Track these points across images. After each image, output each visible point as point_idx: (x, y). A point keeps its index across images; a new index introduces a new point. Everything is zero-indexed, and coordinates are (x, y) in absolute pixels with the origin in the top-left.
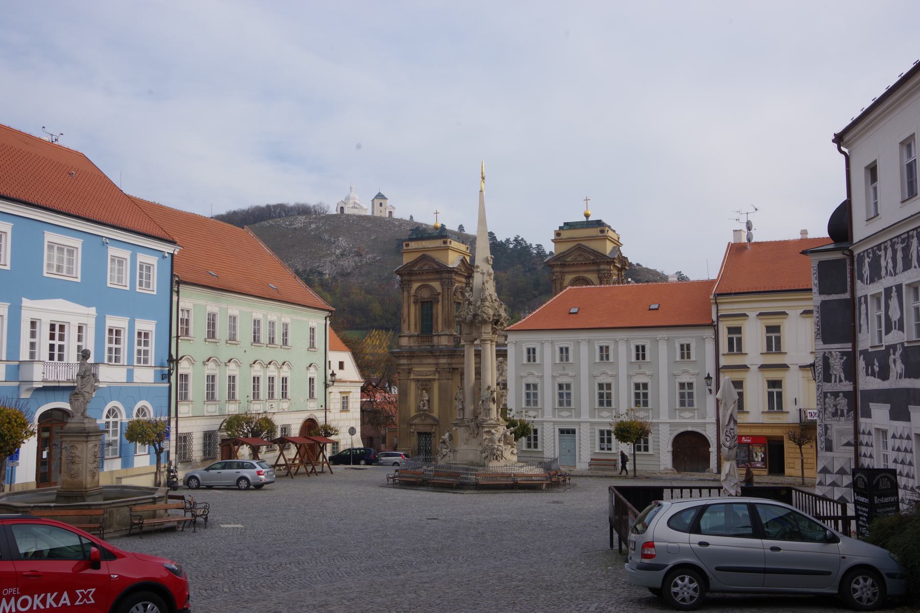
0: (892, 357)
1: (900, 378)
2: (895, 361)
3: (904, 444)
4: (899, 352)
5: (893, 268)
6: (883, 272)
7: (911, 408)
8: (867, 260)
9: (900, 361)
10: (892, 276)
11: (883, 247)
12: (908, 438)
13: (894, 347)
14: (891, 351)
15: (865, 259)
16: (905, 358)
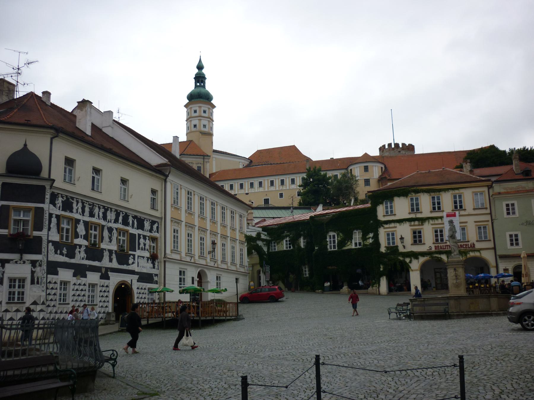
0: (78, 250)
1: (82, 259)
2: (80, 252)
3: (81, 287)
4: (83, 249)
5: (82, 212)
6: (74, 210)
7: (87, 272)
8: (60, 199)
9: (84, 252)
10: (81, 215)
11: (75, 199)
12: (84, 285)
13: (80, 246)
14: (78, 247)
15: (59, 197)
16: (86, 252)
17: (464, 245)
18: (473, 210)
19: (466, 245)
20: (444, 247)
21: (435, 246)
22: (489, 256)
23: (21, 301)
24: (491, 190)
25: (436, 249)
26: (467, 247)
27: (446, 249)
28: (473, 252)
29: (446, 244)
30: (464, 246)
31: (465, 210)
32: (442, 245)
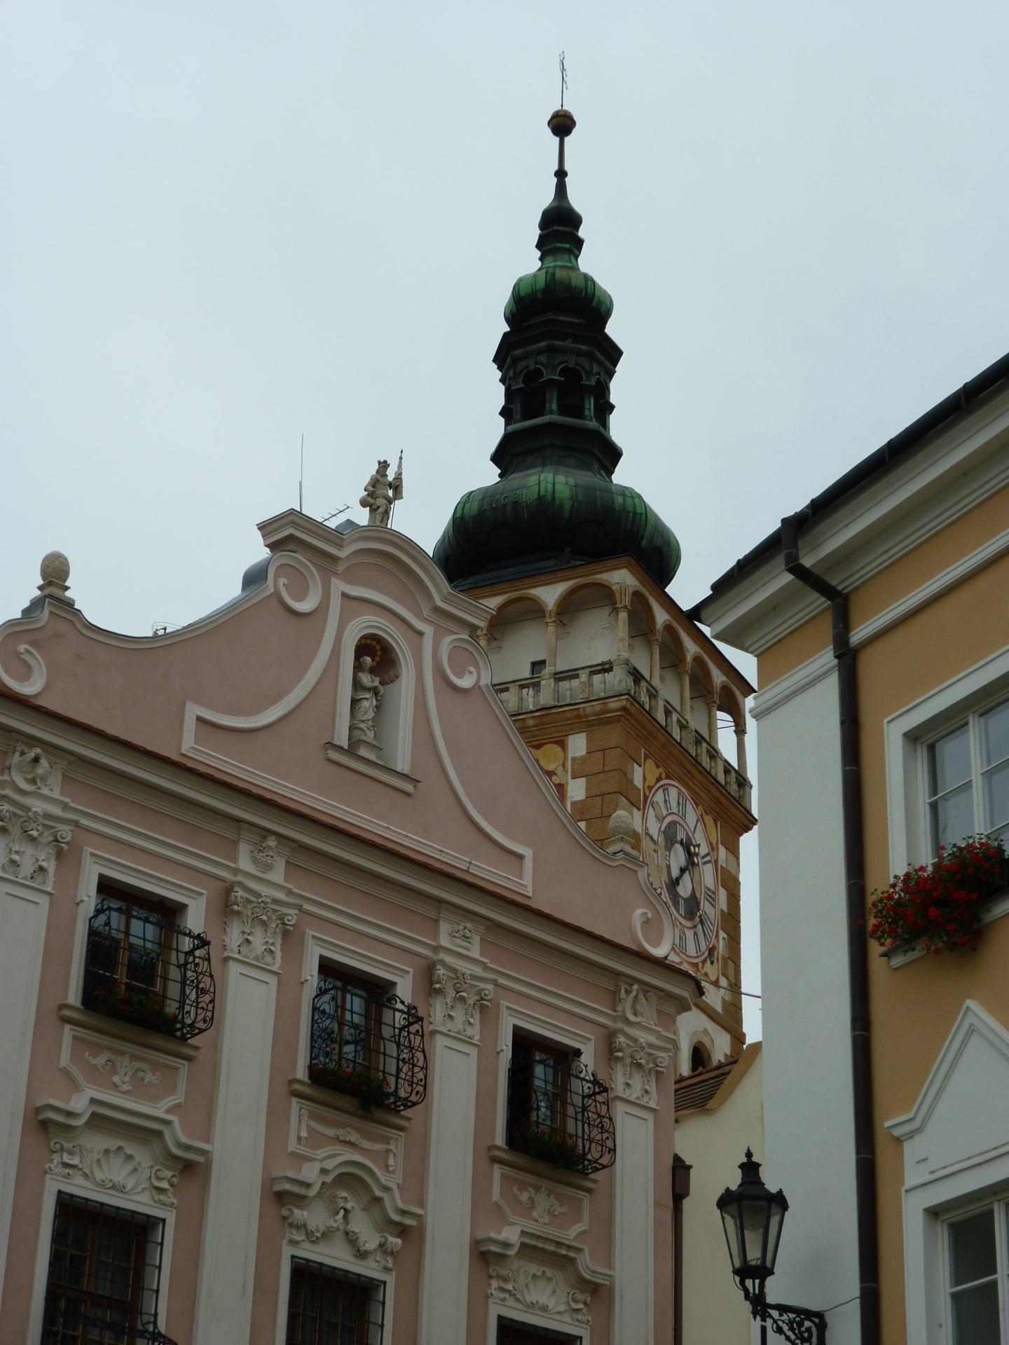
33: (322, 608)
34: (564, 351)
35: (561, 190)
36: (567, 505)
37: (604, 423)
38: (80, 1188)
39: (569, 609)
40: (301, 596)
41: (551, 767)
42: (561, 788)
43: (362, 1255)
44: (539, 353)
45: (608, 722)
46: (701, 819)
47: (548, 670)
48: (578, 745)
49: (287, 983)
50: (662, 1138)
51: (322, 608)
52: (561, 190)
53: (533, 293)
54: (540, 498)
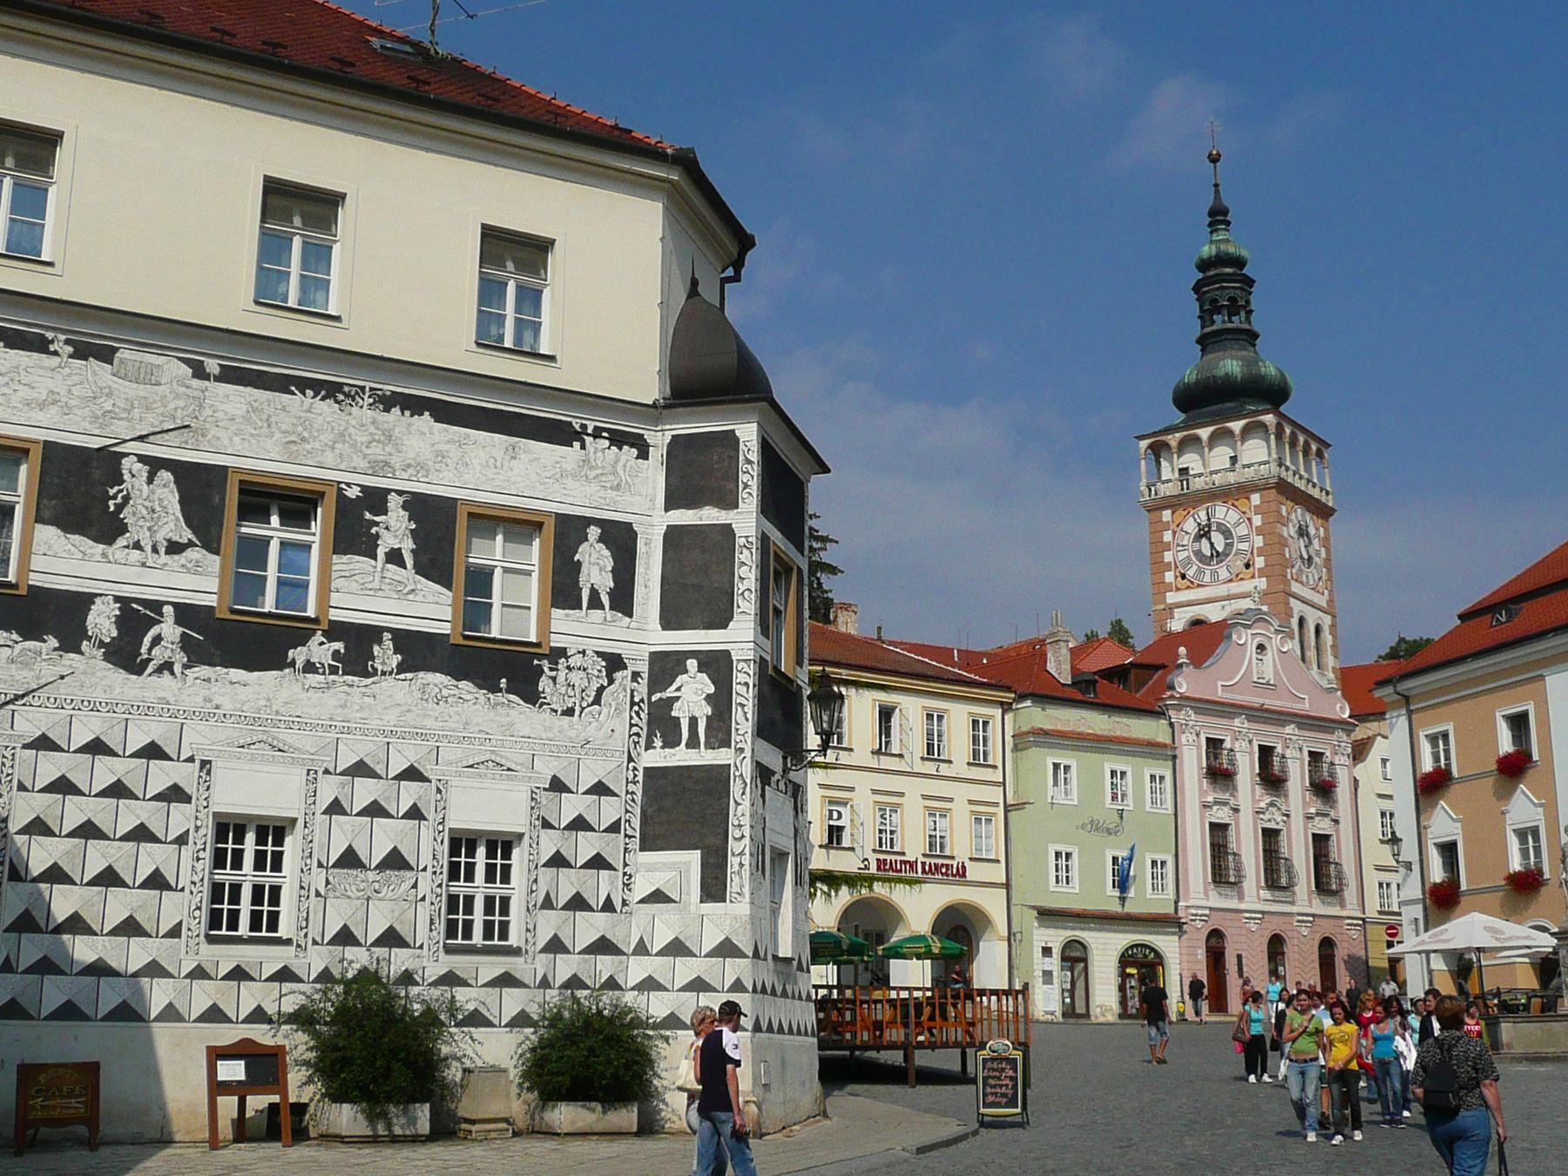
17: (942, 865)
18: (966, 766)
19: (947, 865)
20: (899, 867)
21: (878, 860)
22: (992, 904)
23: (499, 940)
24: (1009, 717)
25: (879, 869)
26: (950, 872)
27: (904, 874)
28: (887, 884)
29: (899, 858)
30: (944, 870)
31: (950, 762)
32: (894, 858)
33: (1246, 640)
34: (1228, 288)
35: (1217, 192)
36: (1239, 376)
37: (1248, 320)
38: (1213, 820)
39: (1246, 432)
40: (1240, 639)
41: (1244, 510)
42: (1249, 519)
43: (1278, 823)
44: (1217, 289)
45: (1269, 488)
46: (1311, 518)
47: (1238, 466)
48: (1256, 499)
49: (1251, 753)
50: (1350, 773)
51: (1246, 640)
52: (1217, 192)
53: (1210, 258)
54: (1227, 374)
